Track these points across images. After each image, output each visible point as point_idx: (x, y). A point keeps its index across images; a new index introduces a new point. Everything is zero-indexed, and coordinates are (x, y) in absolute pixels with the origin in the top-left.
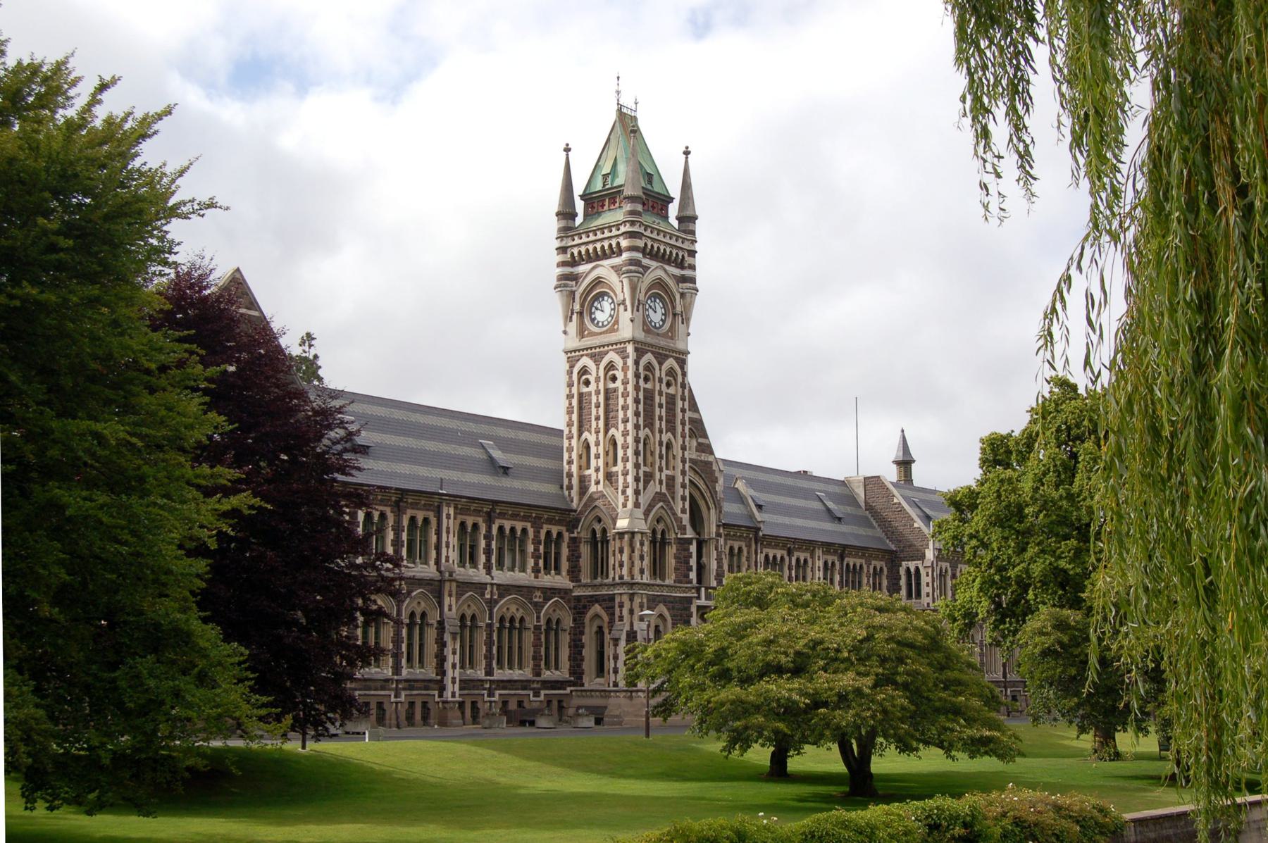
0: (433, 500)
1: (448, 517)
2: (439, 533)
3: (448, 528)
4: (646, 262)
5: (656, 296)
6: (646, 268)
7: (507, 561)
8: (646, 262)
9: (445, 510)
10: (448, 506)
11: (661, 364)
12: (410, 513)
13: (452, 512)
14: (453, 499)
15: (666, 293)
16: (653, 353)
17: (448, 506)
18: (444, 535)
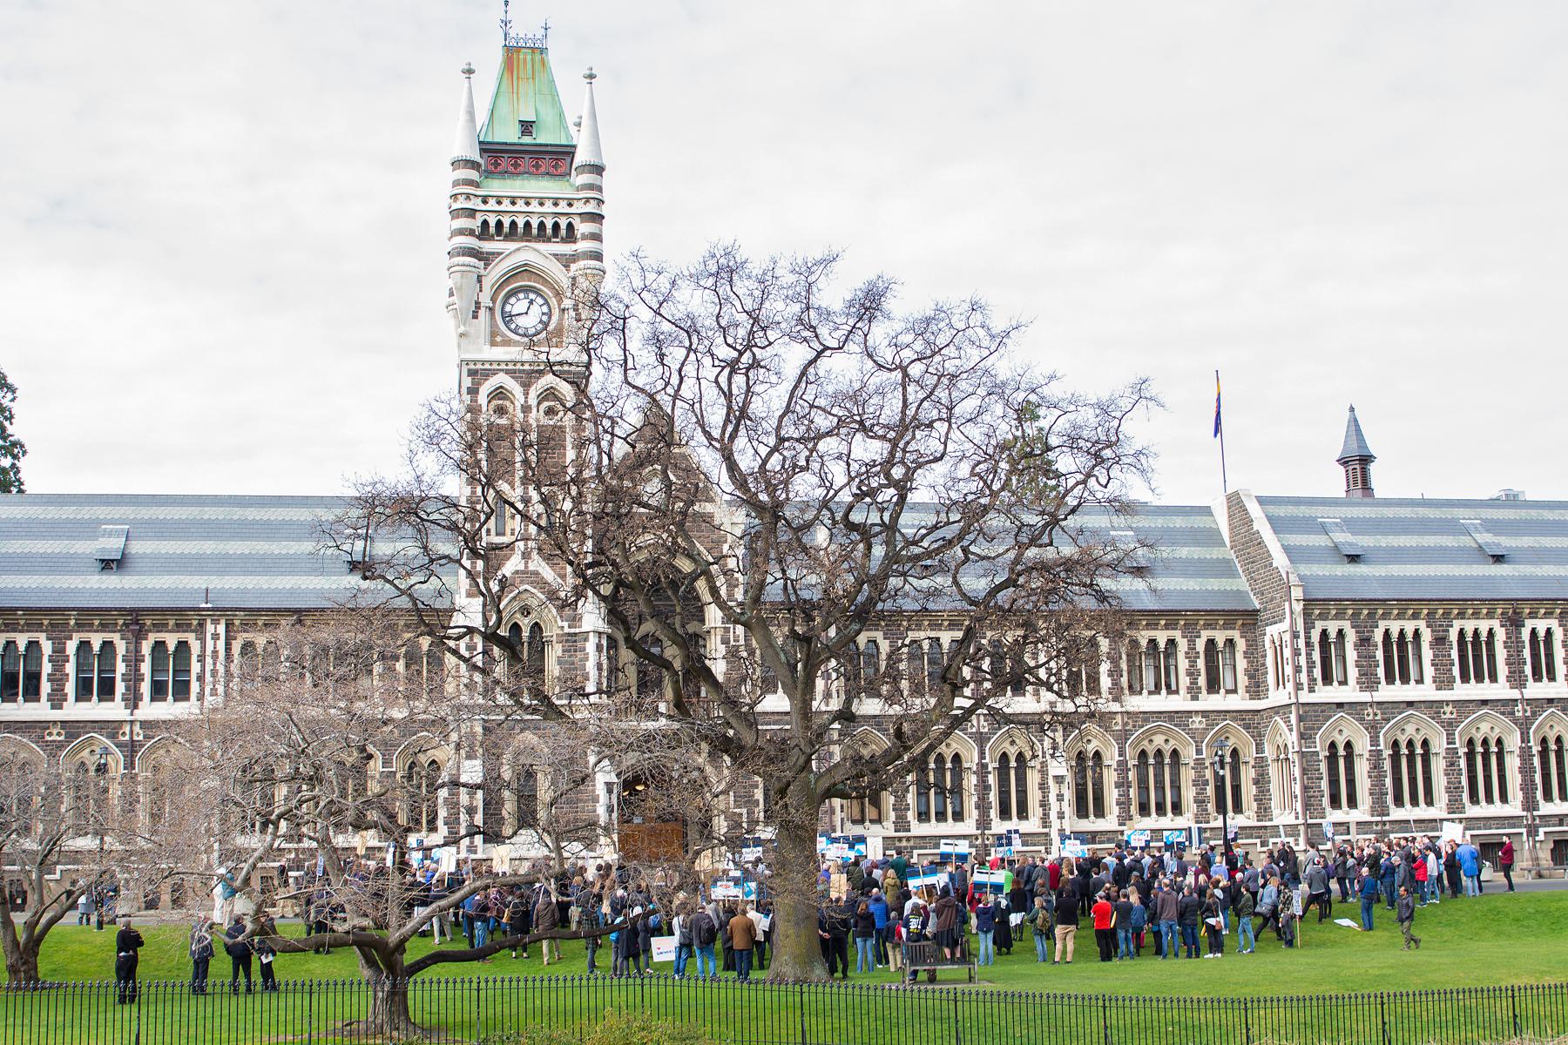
0: (185, 617)
1: (216, 637)
2: (201, 659)
3: (215, 652)
4: (488, 246)
5: (527, 290)
6: (486, 258)
7: (1149, 678)
8: (488, 246)
9: (210, 628)
10: (216, 622)
11: (526, 386)
12: (153, 637)
13: (221, 629)
14: (219, 612)
15: (545, 282)
16: (507, 372)
17: (216, 622)
18: (209, 660)
